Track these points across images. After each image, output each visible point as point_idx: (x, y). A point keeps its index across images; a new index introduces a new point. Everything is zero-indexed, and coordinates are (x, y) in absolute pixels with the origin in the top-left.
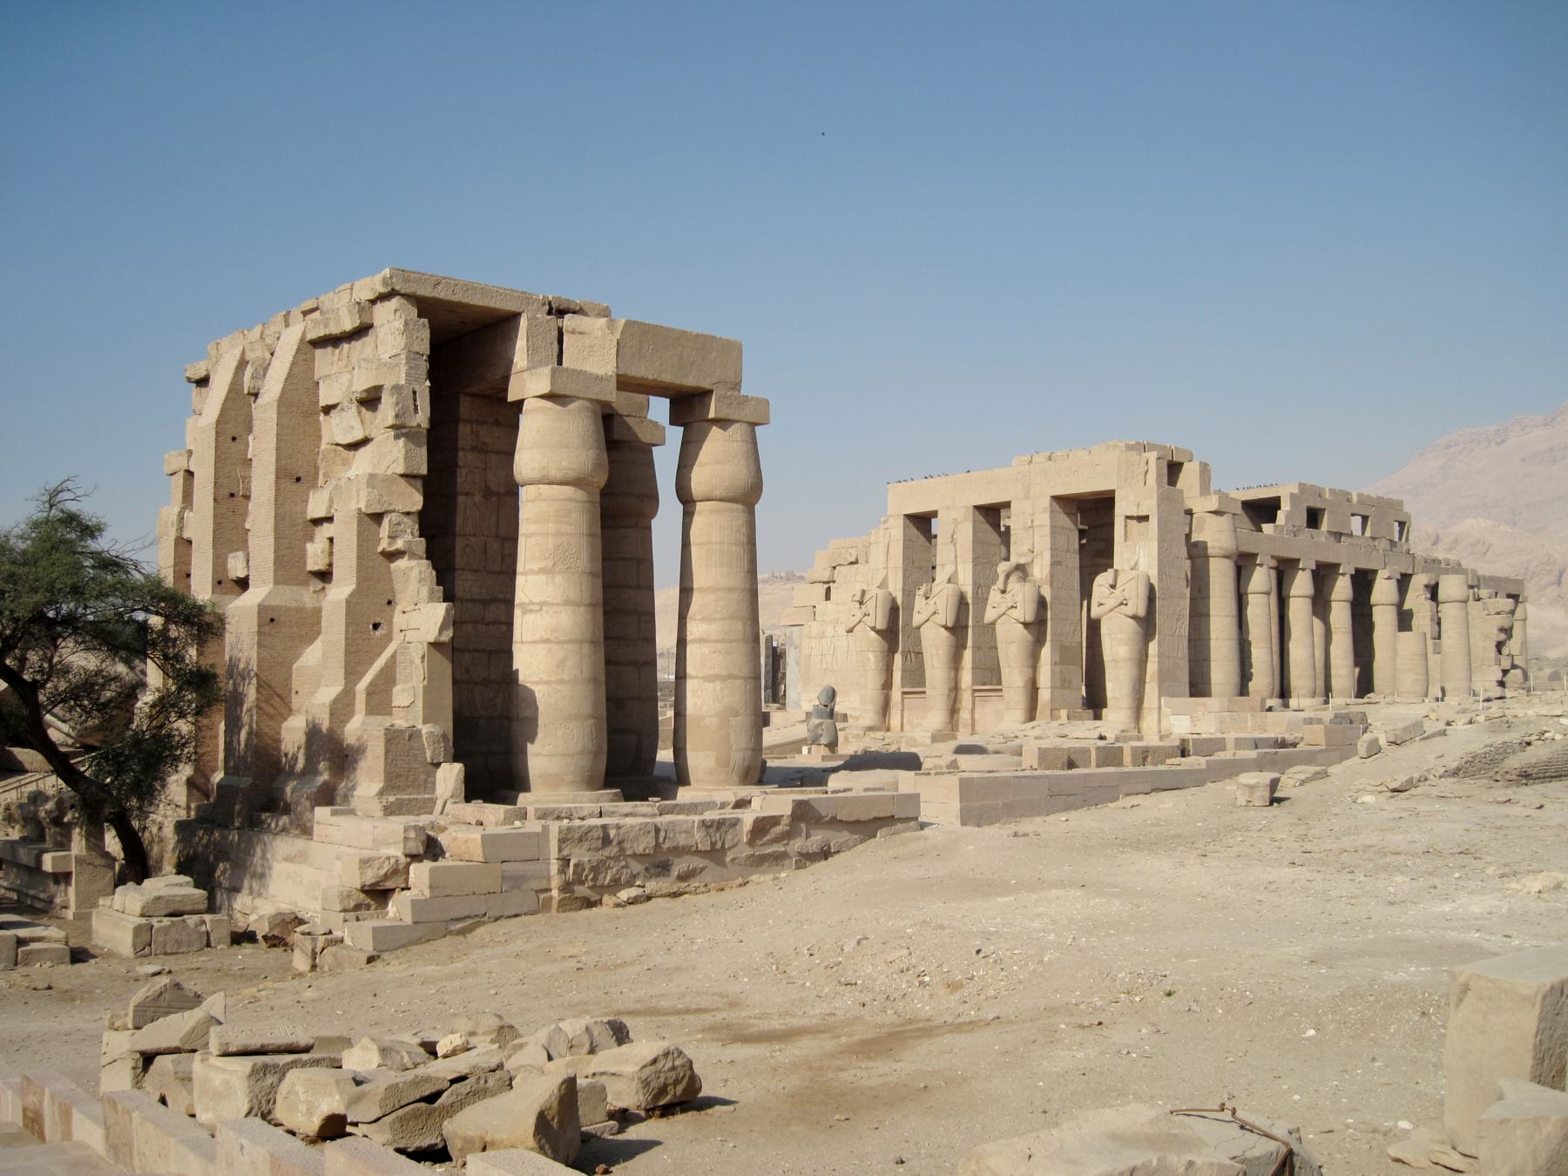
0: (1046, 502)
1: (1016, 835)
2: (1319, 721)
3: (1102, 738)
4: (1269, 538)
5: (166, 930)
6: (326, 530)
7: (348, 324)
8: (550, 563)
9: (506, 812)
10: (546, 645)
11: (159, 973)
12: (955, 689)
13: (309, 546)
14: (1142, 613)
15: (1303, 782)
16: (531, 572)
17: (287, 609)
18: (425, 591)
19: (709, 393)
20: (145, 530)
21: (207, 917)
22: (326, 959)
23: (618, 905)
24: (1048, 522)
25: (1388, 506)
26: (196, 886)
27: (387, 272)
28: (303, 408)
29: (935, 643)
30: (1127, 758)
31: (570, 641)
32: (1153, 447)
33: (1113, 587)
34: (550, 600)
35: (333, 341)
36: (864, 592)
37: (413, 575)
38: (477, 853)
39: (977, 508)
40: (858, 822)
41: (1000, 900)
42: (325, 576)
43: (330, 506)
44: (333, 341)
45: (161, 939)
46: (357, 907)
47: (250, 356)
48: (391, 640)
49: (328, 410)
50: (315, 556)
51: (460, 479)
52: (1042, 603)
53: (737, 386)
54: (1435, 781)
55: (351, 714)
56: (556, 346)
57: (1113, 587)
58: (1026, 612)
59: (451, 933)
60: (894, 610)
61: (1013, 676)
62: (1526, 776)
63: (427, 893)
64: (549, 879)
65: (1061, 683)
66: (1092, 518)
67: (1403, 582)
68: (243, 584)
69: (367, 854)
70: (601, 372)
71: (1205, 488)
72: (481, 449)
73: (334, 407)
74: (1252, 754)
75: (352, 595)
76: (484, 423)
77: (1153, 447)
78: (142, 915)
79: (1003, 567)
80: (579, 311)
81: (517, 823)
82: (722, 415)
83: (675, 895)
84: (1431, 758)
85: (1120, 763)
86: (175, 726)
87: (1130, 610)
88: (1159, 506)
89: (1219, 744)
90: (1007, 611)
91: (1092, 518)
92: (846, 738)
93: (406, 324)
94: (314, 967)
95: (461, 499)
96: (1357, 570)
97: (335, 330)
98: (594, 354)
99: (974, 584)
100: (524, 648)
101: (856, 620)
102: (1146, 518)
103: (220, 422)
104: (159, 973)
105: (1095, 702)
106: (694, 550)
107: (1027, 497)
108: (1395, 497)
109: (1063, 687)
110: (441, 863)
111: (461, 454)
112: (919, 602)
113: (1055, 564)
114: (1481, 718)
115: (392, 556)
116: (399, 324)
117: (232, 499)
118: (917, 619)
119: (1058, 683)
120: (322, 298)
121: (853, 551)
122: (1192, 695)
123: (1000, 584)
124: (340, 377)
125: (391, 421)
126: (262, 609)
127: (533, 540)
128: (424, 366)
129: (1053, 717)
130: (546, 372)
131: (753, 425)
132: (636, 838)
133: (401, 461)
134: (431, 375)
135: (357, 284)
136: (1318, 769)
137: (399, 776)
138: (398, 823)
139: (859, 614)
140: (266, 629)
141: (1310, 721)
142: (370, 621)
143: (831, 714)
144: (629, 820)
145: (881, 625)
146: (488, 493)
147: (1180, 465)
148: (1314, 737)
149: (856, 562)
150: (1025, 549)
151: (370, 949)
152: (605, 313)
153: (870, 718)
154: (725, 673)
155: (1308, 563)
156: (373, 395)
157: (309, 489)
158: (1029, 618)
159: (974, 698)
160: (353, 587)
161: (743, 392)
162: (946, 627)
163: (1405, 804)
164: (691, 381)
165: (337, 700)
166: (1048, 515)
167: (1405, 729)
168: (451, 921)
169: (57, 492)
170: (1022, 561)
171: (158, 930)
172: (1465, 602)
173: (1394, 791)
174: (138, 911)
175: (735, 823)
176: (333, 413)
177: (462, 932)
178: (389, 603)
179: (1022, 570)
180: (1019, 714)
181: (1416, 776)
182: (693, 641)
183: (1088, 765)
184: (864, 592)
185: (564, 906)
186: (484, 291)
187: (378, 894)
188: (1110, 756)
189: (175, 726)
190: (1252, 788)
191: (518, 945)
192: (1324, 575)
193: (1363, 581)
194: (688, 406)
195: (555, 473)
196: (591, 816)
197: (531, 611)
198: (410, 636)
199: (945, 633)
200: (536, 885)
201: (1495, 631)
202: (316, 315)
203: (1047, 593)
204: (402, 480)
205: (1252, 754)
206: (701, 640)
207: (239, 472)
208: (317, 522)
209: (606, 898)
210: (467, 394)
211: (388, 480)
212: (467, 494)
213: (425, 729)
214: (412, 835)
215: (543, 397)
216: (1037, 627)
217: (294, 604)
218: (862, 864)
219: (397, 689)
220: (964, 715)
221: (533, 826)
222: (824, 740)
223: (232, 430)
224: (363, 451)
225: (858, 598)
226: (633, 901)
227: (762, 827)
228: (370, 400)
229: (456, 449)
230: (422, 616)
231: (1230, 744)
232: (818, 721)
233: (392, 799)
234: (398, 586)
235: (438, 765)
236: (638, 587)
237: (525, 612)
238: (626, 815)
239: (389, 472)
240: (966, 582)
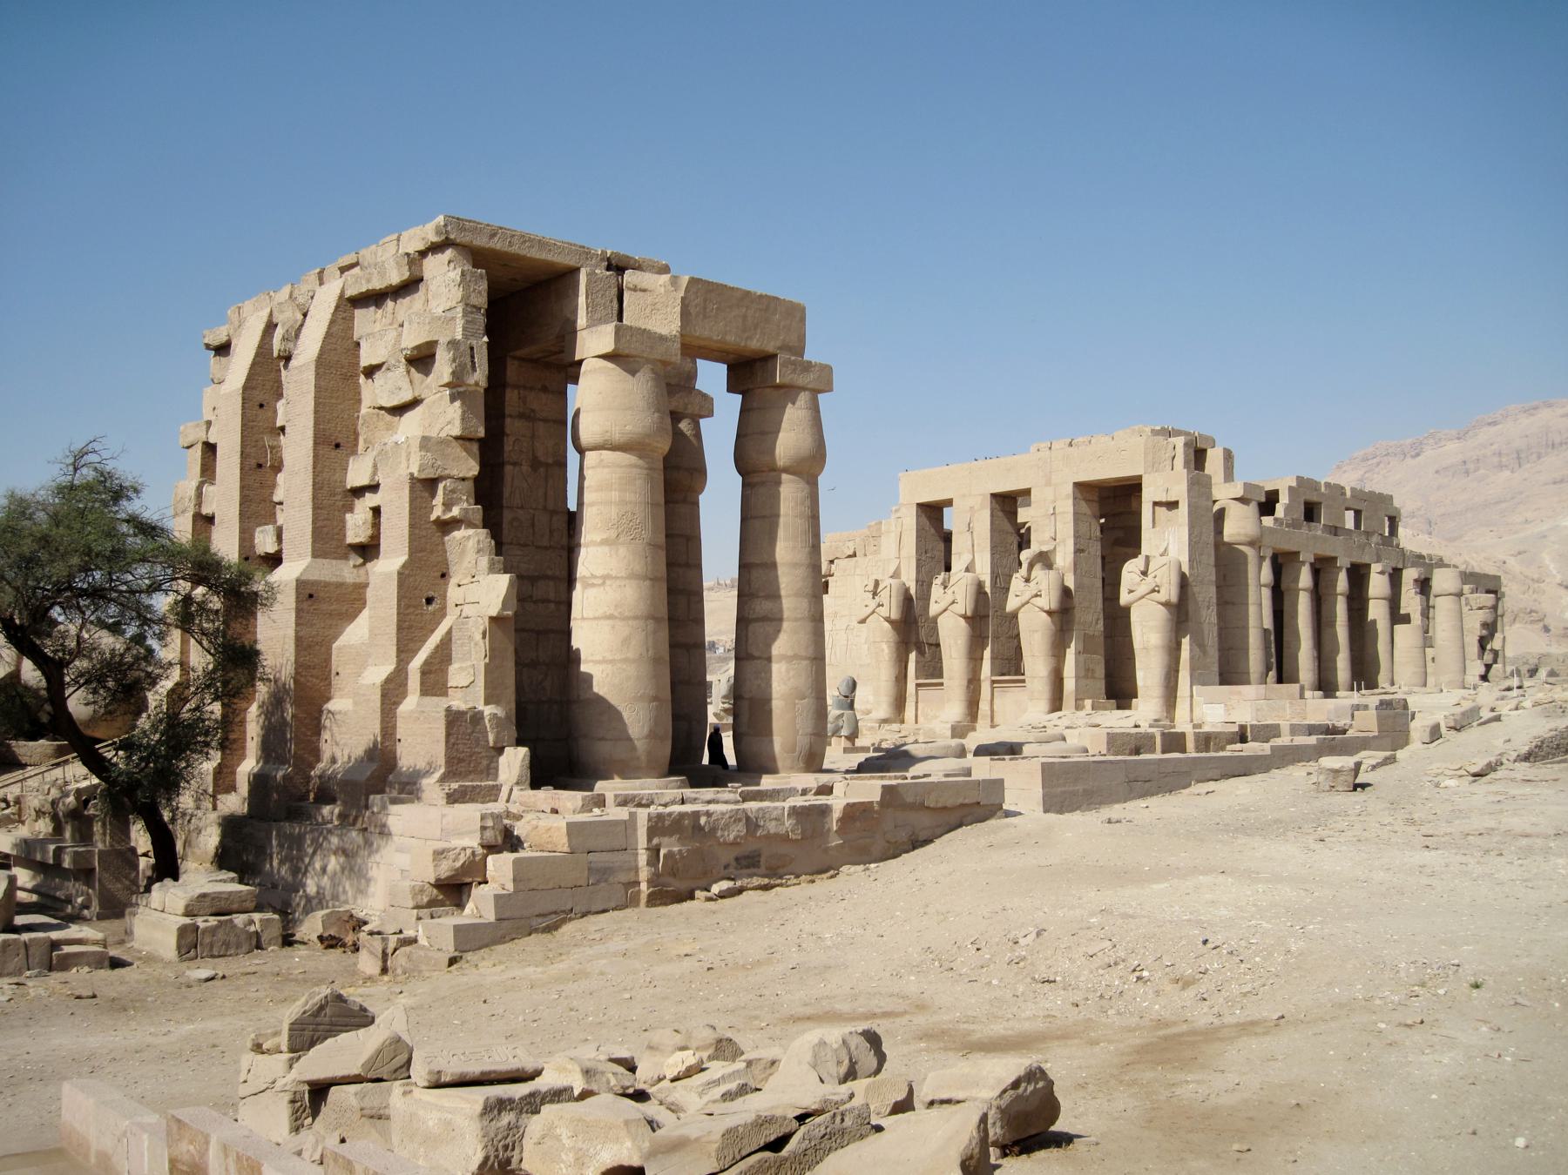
0: (1070, 488)
2: (1366, 707)
5: (212, 931)
6: (370, 500)
7: (395, 277)
8: (613, 533)
9: (584, 799)
10: (610, 622)
11: (213, 978)
12: (973, 683)
13: (348, 516)
14: (1174, 599)
16: (593, 543)
17: (327, 584)
18: (484, 562)
19: (774, 356)
20: (165, 498)
21: (256, 916)
22: (399, 960)
23: (709, 899)
24: (1071, 509)
25: (1382, 501)
26: (241, 882)
27: (440, 219)
28: (342, 368)
29: (952, 635)
30: (1190, 744)
31: (636, 618)
32: (1178, 433)
33: (1145, 573)
34: (614, 573)
35: (374, 299)
36: (877, 583)
37: (469, 547)
38: (563, 844)
39: (994, 496)
40: (945, 808)
41: (1155, 886)
42: (368, 550)
43: (375, 473)
44: (374, 299)
45: (207, 940)
46: (432, 903)
47: (277, 318)
48: (444, 615)
49: (370, 371)
50: (356, 526)
51: (508, 448)
52: (1066, 592)
53: (800, 351)
54: (1511, 766)
55: (404, 695)
56: (615, 305)
57: (1145, 573)
58: (1050, 600)
59: (536, 931)
60: (907, 600)
63: (510, 887)
64: (636, 870)
65: (1084, 673)
68: (275, 560)
69: (440, 845)
70: (664, 331)
71: (1229, 476)
72: (528, 416)
73: (378, 367)
74: (1312, 740)
75: (404, 566)
76: (532, 389)
77: (1178, 433)
78: (187, 914)
79: (1025, 555)
80: (638, 267)
81: (596, 811)
82: (787, 380)
83: (766, 888)
85: (1184, 751)
86: (209, 708)
87: (1163, 596)
90: (1031, 600)
93: (463, 274)
94: (384, 970)
95: (508, 469)
97: (377, 284)
98: (657, 309)
99: (992, 572)
100: (585, 624)
101: (869, 610)
102: (1172, 505)
103: (248, 387)
104: (213, 978)
105: (1120, 691)
107: (1048, 483)
109: (1086, 677)
110: (521, 854)
111: (508, 421)
112: (936, 590)
113: (1078, 551)
115: (446, 526)
116: (455, 274)
117: (260, 468)
118: (934, 609)
120: (363, 252)
121: (851, 544)
122: (1221, 684)
123: (1023, 571)
124: (381, 337)
125: (447, 378)
126: (301, 584)
128: (481, 319)
129: (1079, 707)
130: (610, 328)
131: (815, 392)
132: (727, 826)
133: (458, 423)
134: (489, 331)
135: (405, 235)
136: (1388, 753)
137: (460, 760)
138: (470, 812)
139: (873, 604)
140: (305, 605)
141: (1357, 707)
142: (421, 597)
143: (851, 706)
144: (712, 807)
145: (895, 615)
146: (536, 464)
147: (1204, 451)
148: (1368, 723)
149: (854, 555)
150: (1048, 535)
151: (450, 949)
152: (665, 270)
153: (883, 710)
154: (790, 653)
156: (425, 352)
157: (348, 456)
159: (993, 689)
160: (405, 557)
161: (806, 357)
162: (965, 617)
163: (1493, 788)
164: (755, 344)
165: (388, 680)
166: (1070, 501)
167: (1463, 714)
168: (538, 912)
169: (83, 453)
170: (1044, 549)
171: (206, 930)
172: (1460, 595)
173: (1475, 775)
174: (181, 910)
175: (825, 811)
176: (377, 376)
177: (549, 929)
178: (443, 576)
180: (1043, 704)
183: (1153, 751)
184: (877, 583)
185: (653, 900)
186: (542, 244)
187: (453, 890)
188: (1139, 744)
189: (209, 708)
190: (1336, 772)
191: (617, 944)
194: (747, 372)
195: (617, 437)
196: (673, 802)
197: (593, 585)
198: (468, 610)
199: (962, 621)
200: (623, 877)
202: (356, 270)
203: (1070, 582)
204: (455, 443)
207: (268, 441)
208: (358, 492)
209: (698, 893)
210: (514, 358)
211: (442, 442)
212: (515, 464)
213: (488, 710)
214: (490, 823)
215: (605, 357)
216: (1064, 614)
217: (334, 579)
218: (956, 852)
219: (453, 669)
220: (984, 706)
221: (622, 814)
222: (844, 732)
223: (259, 396)
224: (409, 416)
225: (871, 588)
226: (722, 895)
227: (854, 813)
228: (421, 359)
229: (503, 416)
230: (480, 590)
231: (1285, 729)
232: (839, 712)
233: (455, 786)
234: (452, 557)
235: (500, 750)
236: (687, 565)
237: (587, 586)
238: (709, 802)
239: (443, 435)
240: (984, 572)
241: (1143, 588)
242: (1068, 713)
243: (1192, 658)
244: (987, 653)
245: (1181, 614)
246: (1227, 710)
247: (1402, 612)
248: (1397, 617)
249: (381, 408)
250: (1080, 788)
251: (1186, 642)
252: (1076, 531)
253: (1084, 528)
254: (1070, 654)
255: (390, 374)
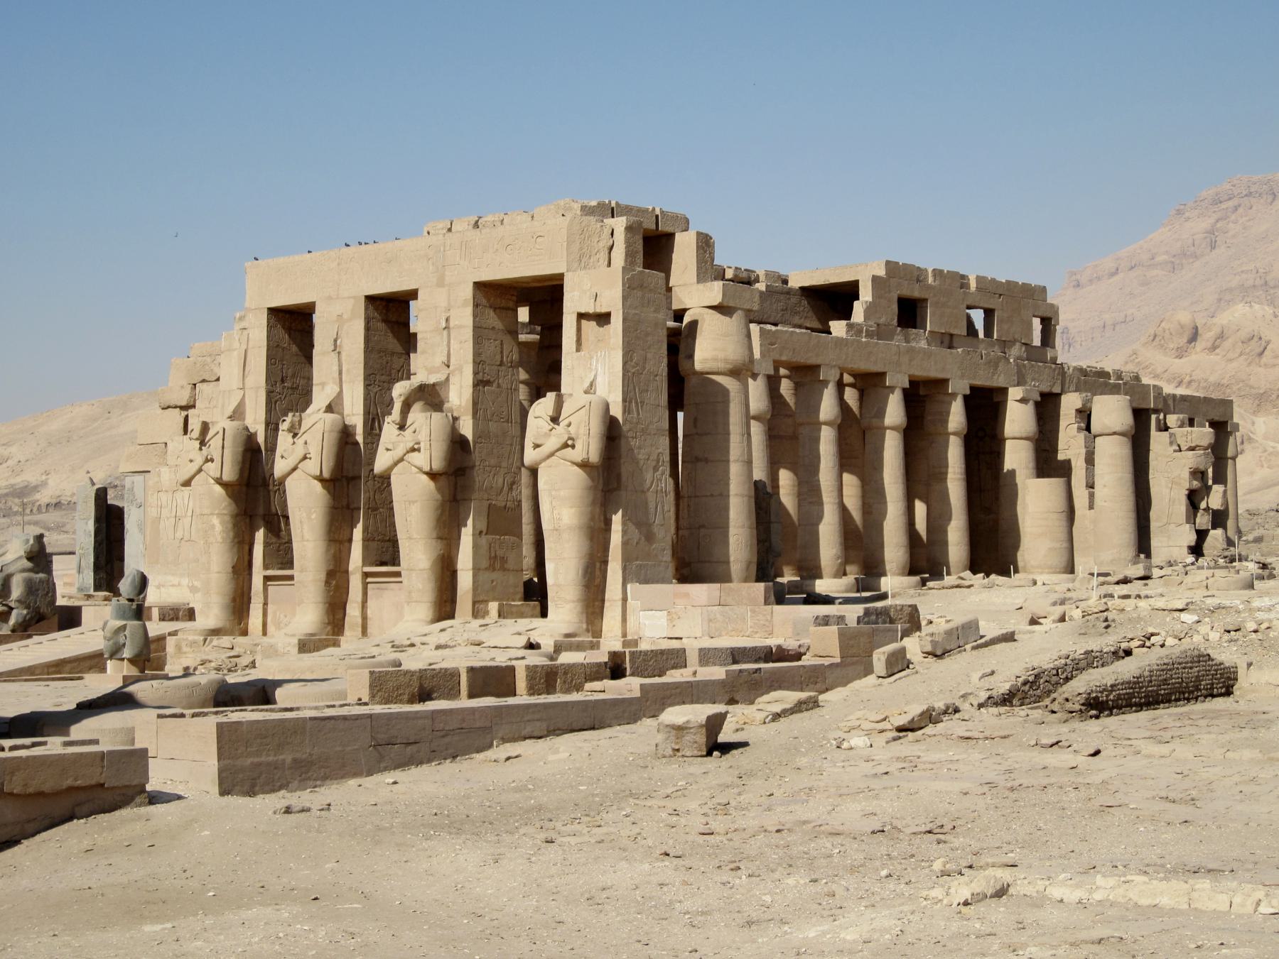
0: (468, 292)
1: (288, 810)
3: (531, 646)
4: (839, 341)
14: (594, 457)
15: (777, 717)
24: (469, 321)
25: (1028, 297)
29: (305, 504)
30: (521, 683)
33: (555, 420)
39: (371, 300)
40: (40, 794)
52: (458, 444)
61: (417, 551)
62: (1097, 706)
66: (527, 319)
67: (1046, 408)
84: (975, 677)
87: (578, 454)
88: (625, 298)
89: (676, 658)
90: (408, 457)
91: (527, 319)
92: (178, 647)
96: (972, 388)
99: (367, 412)
101: (193, 468)
102: (603, 319)
107: (441, 283)
108: (1034, 281)
109: (492, 568)
112: (284, 439)
114: (1077, 614)
119: (485, 563)
122: (683, 579)
129: (476, 615)
139: (199, 460)
145: (229, 474)
150: (440, 358)
153: (211, 613)
155: (898, 380)
158: (437, 465)
162: (320, 479)
166: (469, 310)
167: (949, 633)
170: (432, 379)
179: (430, 396)
181: (940, 705)
183: (453, 693)
190: (680, 729)
192: (922, 398)
193: (985, 407)
199: (318, 486)
201: (1186, 474)
205: (717, 673)
220: (353, 611)
222: (127, 653)
231: (692, 658)
232: (120, 623)
240: (355, 414)
241: (552, 443)
242: (463, 625)
243: (625, 543)
244: (358, 533)
245: (609, 475)
246: (670, 620)
247: (1061, 457)
248: (1048, 462)
250: (287, 757)
251: (617, 519)
252: (477, 354)
253: (491, 348)
254: (467, 535)
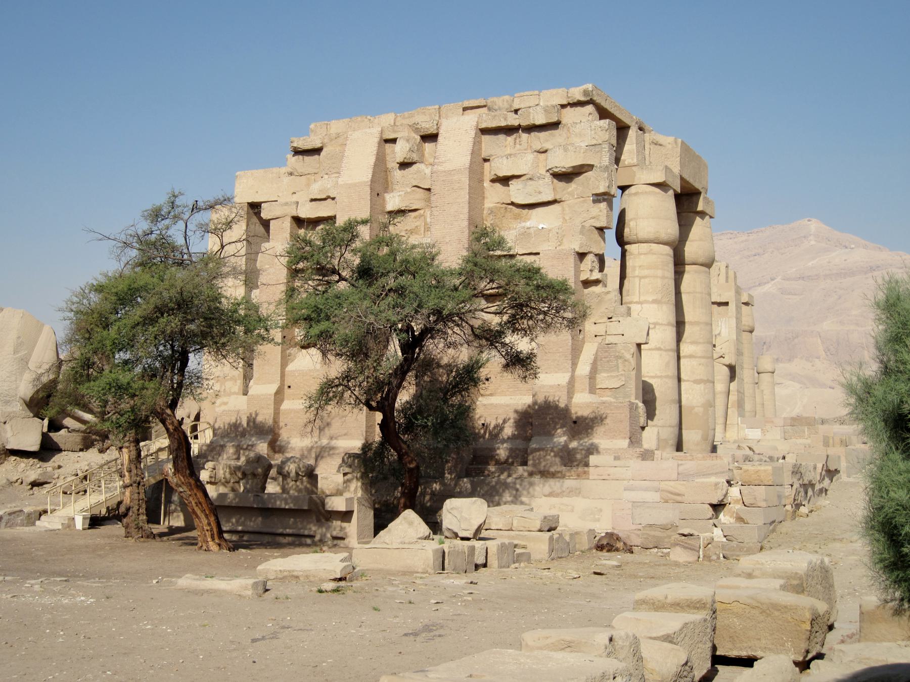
7: (540, 120)
10: (660, 352)
34: (660, 321)
102: (726, 304)
106: (685, 298)
127: (647, 280)
182: (685, 357)
195: (664, 236)
206: (691, 356)
249: (513, 204)
255: (531, 182)
